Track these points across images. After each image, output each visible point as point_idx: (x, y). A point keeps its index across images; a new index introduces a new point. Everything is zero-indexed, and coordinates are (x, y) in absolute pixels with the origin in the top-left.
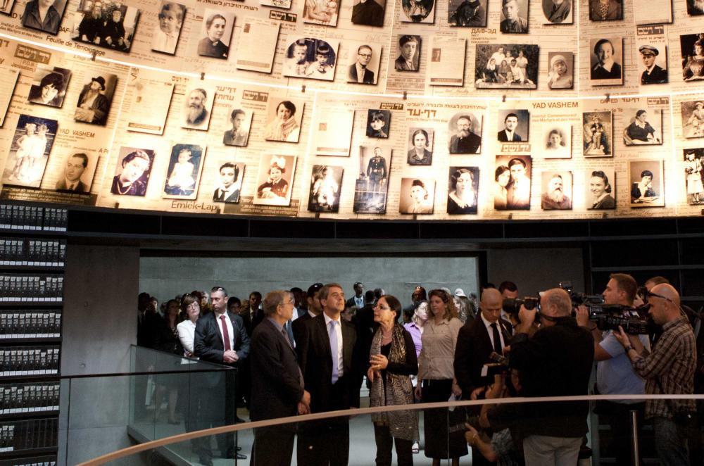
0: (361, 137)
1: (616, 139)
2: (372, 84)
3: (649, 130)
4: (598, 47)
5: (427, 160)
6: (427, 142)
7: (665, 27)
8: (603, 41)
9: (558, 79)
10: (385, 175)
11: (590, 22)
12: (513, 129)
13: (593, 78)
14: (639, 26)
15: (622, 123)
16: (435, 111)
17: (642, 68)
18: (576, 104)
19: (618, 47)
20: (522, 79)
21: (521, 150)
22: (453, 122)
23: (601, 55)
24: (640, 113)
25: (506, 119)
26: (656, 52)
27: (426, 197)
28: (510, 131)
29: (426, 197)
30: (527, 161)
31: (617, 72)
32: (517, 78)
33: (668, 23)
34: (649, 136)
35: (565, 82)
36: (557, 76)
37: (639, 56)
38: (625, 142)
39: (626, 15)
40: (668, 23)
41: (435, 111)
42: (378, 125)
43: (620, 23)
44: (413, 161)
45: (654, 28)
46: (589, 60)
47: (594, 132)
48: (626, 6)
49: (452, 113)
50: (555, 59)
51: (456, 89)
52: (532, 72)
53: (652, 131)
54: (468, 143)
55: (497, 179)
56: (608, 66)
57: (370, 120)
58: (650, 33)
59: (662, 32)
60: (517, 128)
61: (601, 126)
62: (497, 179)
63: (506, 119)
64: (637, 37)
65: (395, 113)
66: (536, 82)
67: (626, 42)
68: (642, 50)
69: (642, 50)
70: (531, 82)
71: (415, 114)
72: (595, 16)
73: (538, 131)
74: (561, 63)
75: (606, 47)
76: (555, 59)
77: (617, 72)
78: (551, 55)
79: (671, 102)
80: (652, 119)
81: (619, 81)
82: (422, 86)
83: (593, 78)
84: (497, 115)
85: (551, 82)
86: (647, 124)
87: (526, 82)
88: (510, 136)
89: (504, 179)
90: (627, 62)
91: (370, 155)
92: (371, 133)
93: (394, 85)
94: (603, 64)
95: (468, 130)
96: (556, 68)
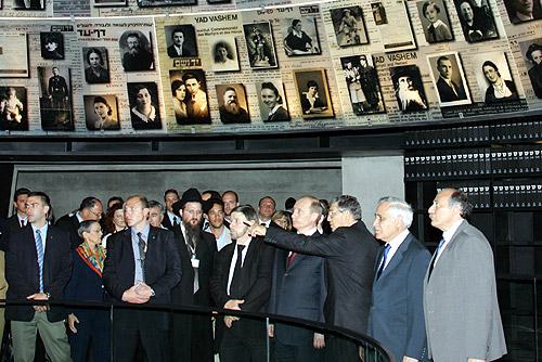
0: (38, 60)
1: (278, 50)
2: (39, 8)
3: (306, 39)
5: (105, 78)
6: (102, 60)
10: (66, 94)
15: (281, 33)
16: (104, 31)
18: (235, 17)
21: (192, 64)
22: (123, 41)
24: (296, 22)
25: (173, 34)
27: (109, 113)
28: (179, 46)
29: (109, 113)
30: (200, 76)
34: (307, 45)
38: (287, 53)
41: (104, 31)
42: (53, 47)
44: (92, 79)
47: (257, 44)
49: (120, 32)
51: (120, 9)
53: (309, 41)
54: (139, 58)
55: (174, 94)
57: (43, 43)
61: (262, 38)
62: (174, 94)
63: (173, 34)
65: (67, 35)
71: (85, 35)
73: (205, 45)
79: (321, 11)
80: (307, 28)
82: (89, 8)
86: (303, 33)
88: (179, 51)
89: (181, 93)
91: (49, 75)
92: (46, 54)
93: (61, 8)
95: (138, 47)
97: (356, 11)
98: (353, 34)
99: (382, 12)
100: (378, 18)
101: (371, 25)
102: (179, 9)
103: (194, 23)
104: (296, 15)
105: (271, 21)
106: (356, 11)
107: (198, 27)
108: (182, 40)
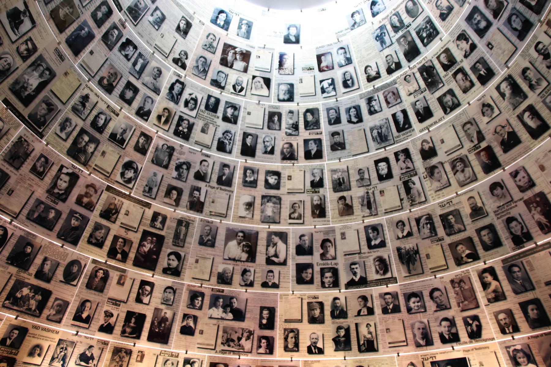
4: (83, 304)
7: (122, 304)
8: (88, 301)
9: (54, 315)
11: (85, 288)
12: (13, 338)
13: (74, 319)
14: (109, 299)
17: (102, 322)
19: (94, 307)
20: (33, 308)
23: (83, 308)
26: (112, 315)
28: (10, 339)
31: (88, 321)
32: (30, 307)
33: (124, 302)
35: (58, 317)
36: (54, 312)
37: (103, 314)
39: (105, 291)
40: (124, 302)
43: (100, 294)
45: (116, 302)
46: (76, 309)
48: (107, 286)
50: (57, 302)
52: (41, 306)
56: (84, 316)
58: (113, 304)
59: (119, 305)
60: (15, 338)
63: (12, 330)
64: (106, 304)
66: (41, 313)
67: (100, 305)
68: (106, 312)
69: (106, 312)
70: (38, 312)
72: (89, 286)
74: (59, 305)
75: (88, 304)
76: (57, 302)
77: (88, 321)
78: (57, 299)
81: (86, 326)
83: (74, 319)
84: (7, 326)
85: (49, 315)
87: (35, 311)
88: (9, 342)
90: (95, 316)
94: (82, 313)
96: (56, 308)
97: (128, 352)
98: (120, 363)
99: (143, 356)
100: (139, 359)
101: (133, 361)
102: (26, 316)
103: (30, 328)
104: (93, 343)
105: (77, 342)
106: (128, 352)
107: (31, 331)
108: (15, 336)
